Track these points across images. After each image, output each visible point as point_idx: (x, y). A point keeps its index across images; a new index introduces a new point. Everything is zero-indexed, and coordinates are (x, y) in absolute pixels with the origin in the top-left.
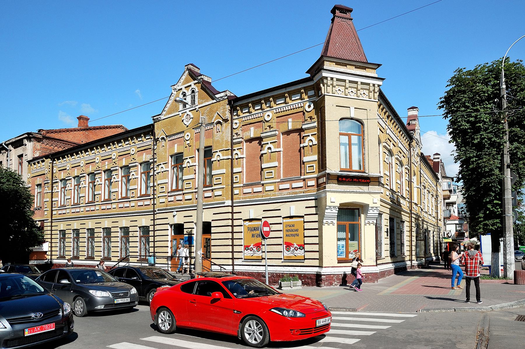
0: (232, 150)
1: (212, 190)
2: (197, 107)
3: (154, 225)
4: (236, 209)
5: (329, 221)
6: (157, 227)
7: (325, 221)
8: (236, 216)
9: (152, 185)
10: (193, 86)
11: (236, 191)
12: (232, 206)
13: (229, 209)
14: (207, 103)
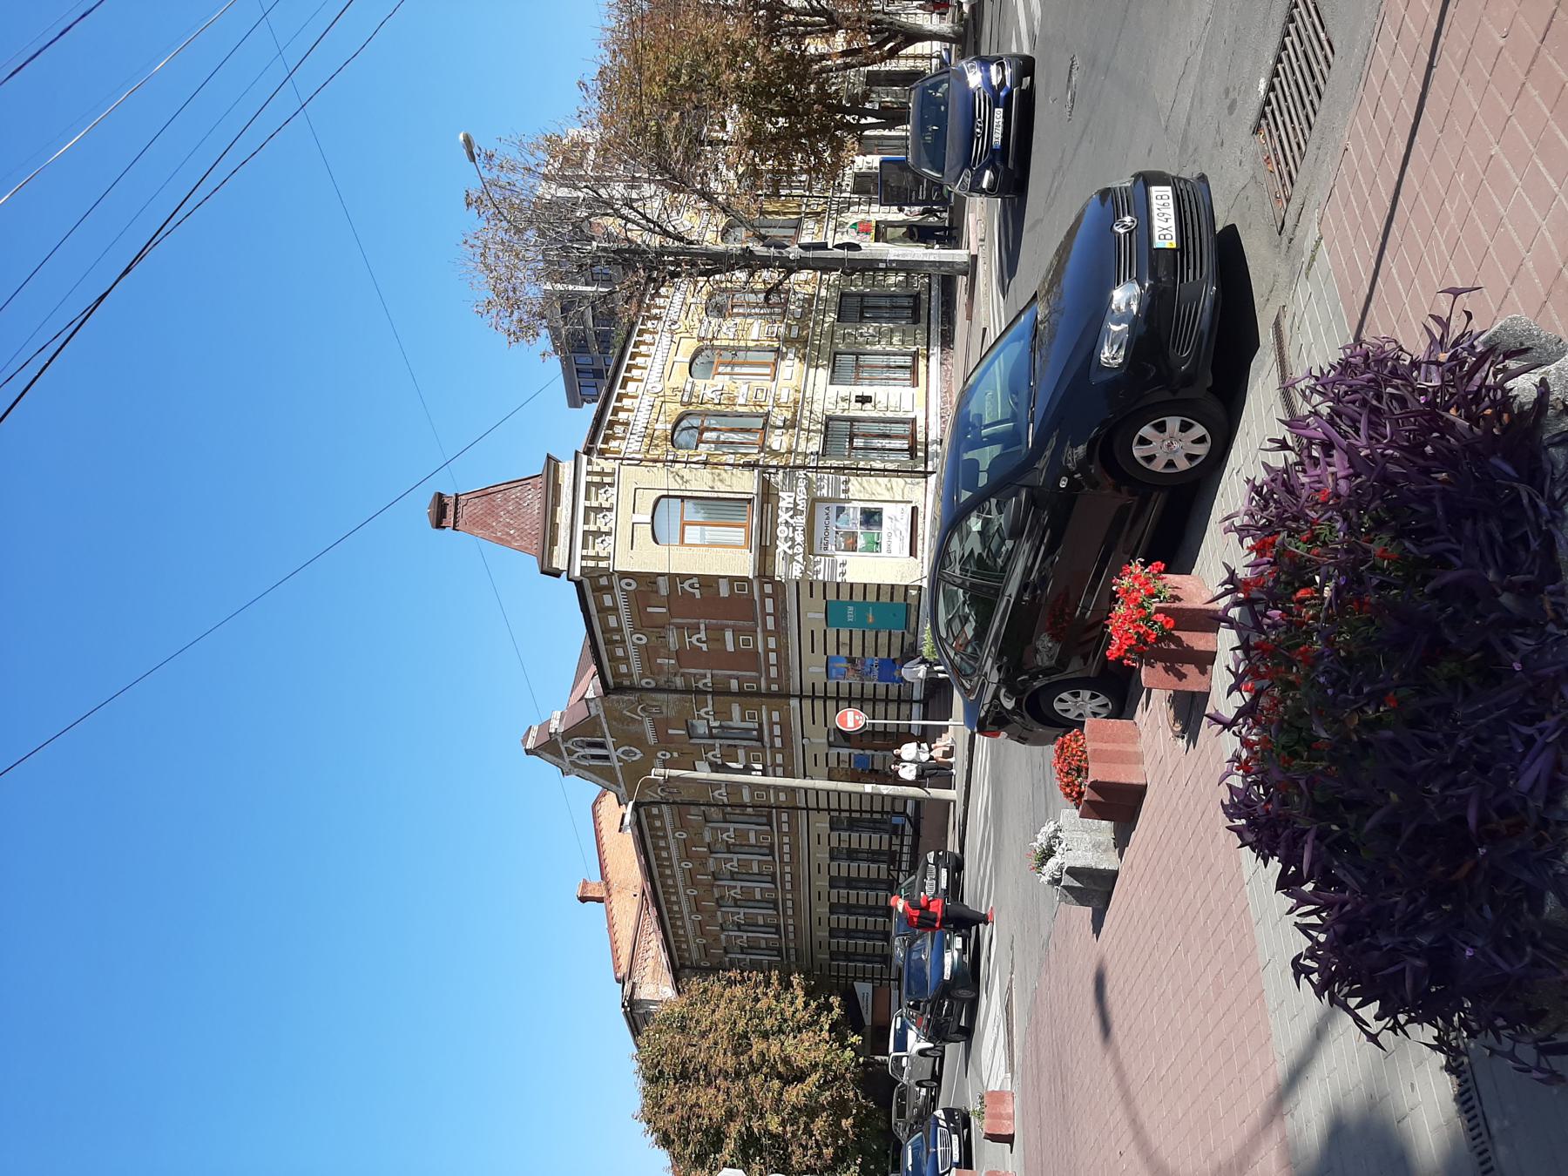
0: (698, 692)
1: (771, 724)
2: (610, 741)
3: (829, 810)
4: (808, 691)
5: (839, 570)
6: (834, 805)
8: (820, 692)
9: (750, 810)
10: (569, 744)
11: (774, 687)
12: (801, 697)
13: (807, 703)
14: (605, 726)
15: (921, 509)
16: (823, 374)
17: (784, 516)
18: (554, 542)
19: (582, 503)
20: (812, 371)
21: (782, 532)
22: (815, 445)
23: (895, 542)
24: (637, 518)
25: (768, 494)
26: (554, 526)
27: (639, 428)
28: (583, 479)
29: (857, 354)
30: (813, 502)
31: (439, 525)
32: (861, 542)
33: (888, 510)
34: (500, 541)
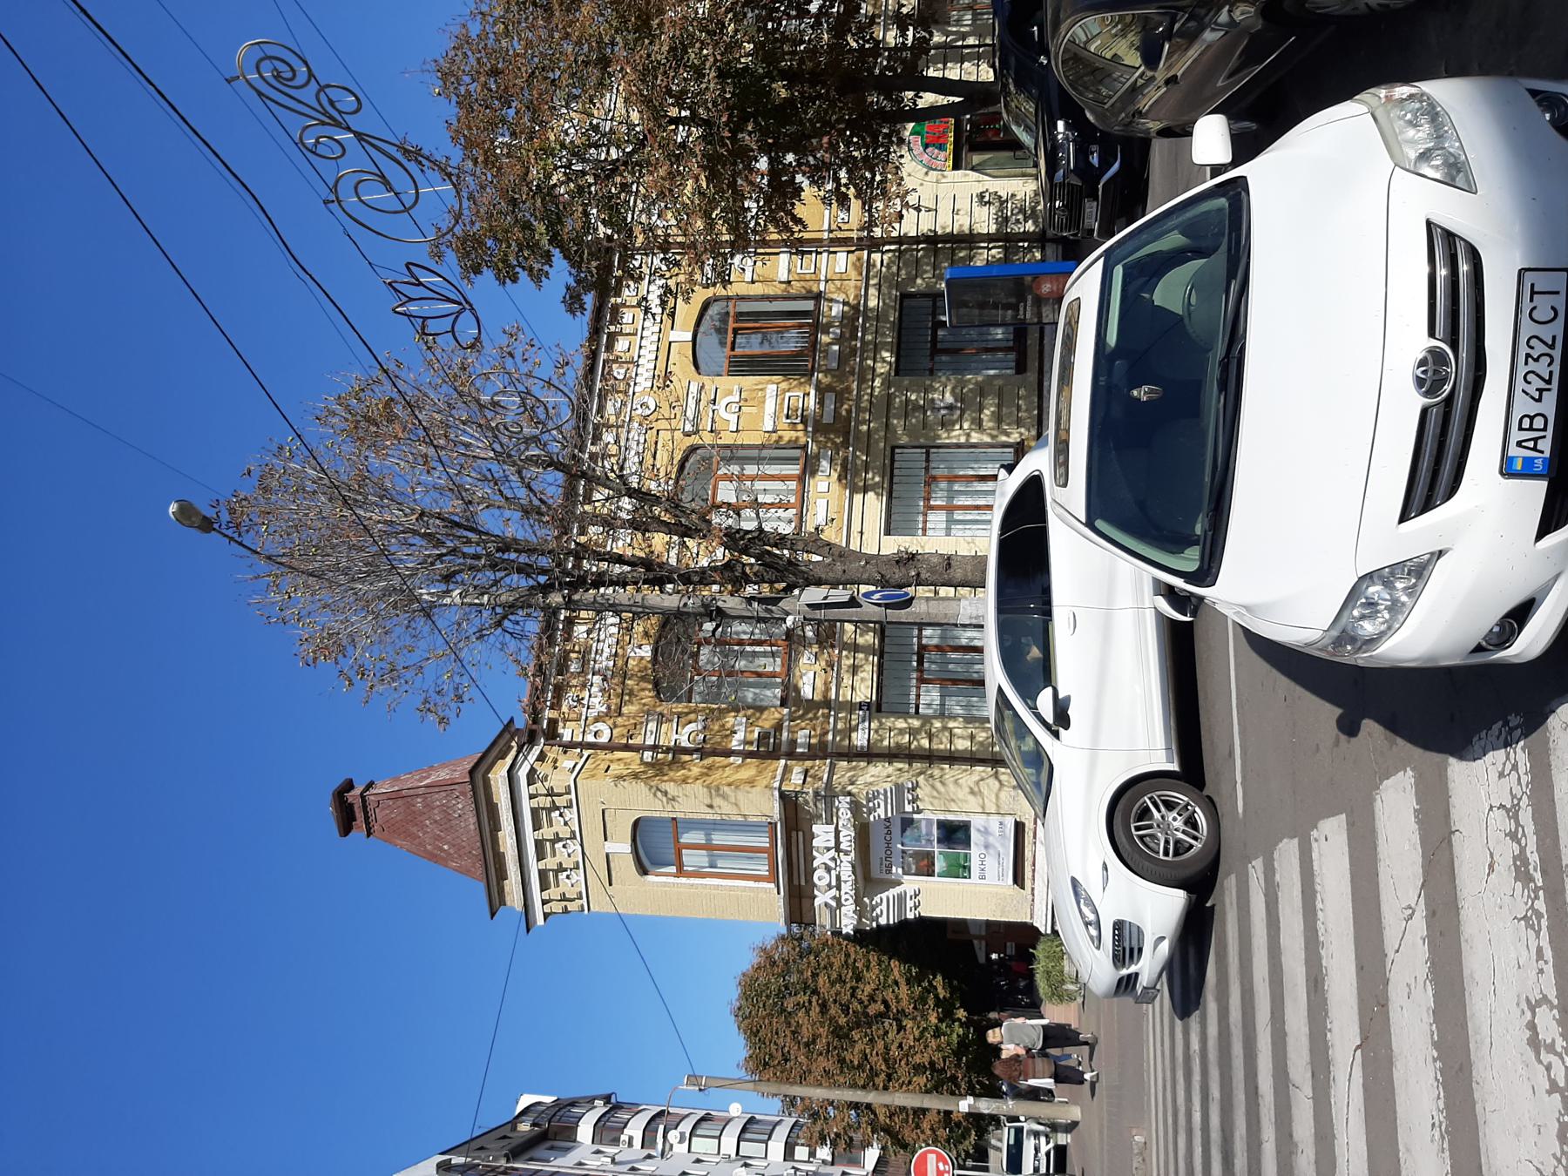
5: (910, 904)
7: (910, 916)
15: (1029, 826)
16: (873, 507)
17: (820, 859)
18: (502, 875)
19: (530, 837)
20: (858, 498)
21: (820, 878)
22: (864, 689)
23: (991, 862)
24: (610, 847)
25: (795, 819)
26: (499, 858)
27: (604, 662)
28: (526, 806)
29: (928, 448)
30: (863, 833)
31: (346, 827)
32: (939, 865)
33: (977, 822)
34: (433, 857)
